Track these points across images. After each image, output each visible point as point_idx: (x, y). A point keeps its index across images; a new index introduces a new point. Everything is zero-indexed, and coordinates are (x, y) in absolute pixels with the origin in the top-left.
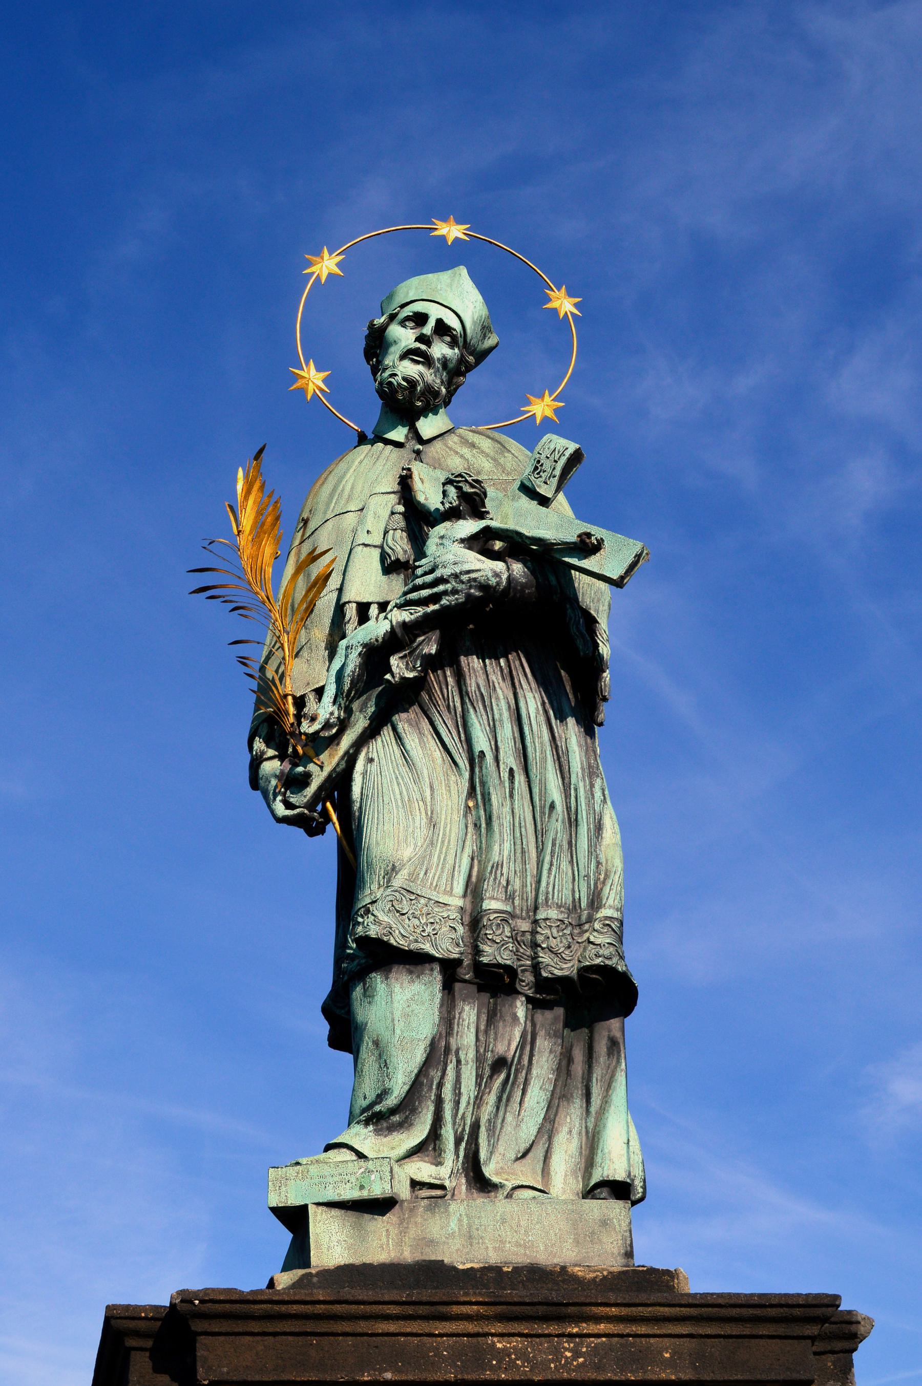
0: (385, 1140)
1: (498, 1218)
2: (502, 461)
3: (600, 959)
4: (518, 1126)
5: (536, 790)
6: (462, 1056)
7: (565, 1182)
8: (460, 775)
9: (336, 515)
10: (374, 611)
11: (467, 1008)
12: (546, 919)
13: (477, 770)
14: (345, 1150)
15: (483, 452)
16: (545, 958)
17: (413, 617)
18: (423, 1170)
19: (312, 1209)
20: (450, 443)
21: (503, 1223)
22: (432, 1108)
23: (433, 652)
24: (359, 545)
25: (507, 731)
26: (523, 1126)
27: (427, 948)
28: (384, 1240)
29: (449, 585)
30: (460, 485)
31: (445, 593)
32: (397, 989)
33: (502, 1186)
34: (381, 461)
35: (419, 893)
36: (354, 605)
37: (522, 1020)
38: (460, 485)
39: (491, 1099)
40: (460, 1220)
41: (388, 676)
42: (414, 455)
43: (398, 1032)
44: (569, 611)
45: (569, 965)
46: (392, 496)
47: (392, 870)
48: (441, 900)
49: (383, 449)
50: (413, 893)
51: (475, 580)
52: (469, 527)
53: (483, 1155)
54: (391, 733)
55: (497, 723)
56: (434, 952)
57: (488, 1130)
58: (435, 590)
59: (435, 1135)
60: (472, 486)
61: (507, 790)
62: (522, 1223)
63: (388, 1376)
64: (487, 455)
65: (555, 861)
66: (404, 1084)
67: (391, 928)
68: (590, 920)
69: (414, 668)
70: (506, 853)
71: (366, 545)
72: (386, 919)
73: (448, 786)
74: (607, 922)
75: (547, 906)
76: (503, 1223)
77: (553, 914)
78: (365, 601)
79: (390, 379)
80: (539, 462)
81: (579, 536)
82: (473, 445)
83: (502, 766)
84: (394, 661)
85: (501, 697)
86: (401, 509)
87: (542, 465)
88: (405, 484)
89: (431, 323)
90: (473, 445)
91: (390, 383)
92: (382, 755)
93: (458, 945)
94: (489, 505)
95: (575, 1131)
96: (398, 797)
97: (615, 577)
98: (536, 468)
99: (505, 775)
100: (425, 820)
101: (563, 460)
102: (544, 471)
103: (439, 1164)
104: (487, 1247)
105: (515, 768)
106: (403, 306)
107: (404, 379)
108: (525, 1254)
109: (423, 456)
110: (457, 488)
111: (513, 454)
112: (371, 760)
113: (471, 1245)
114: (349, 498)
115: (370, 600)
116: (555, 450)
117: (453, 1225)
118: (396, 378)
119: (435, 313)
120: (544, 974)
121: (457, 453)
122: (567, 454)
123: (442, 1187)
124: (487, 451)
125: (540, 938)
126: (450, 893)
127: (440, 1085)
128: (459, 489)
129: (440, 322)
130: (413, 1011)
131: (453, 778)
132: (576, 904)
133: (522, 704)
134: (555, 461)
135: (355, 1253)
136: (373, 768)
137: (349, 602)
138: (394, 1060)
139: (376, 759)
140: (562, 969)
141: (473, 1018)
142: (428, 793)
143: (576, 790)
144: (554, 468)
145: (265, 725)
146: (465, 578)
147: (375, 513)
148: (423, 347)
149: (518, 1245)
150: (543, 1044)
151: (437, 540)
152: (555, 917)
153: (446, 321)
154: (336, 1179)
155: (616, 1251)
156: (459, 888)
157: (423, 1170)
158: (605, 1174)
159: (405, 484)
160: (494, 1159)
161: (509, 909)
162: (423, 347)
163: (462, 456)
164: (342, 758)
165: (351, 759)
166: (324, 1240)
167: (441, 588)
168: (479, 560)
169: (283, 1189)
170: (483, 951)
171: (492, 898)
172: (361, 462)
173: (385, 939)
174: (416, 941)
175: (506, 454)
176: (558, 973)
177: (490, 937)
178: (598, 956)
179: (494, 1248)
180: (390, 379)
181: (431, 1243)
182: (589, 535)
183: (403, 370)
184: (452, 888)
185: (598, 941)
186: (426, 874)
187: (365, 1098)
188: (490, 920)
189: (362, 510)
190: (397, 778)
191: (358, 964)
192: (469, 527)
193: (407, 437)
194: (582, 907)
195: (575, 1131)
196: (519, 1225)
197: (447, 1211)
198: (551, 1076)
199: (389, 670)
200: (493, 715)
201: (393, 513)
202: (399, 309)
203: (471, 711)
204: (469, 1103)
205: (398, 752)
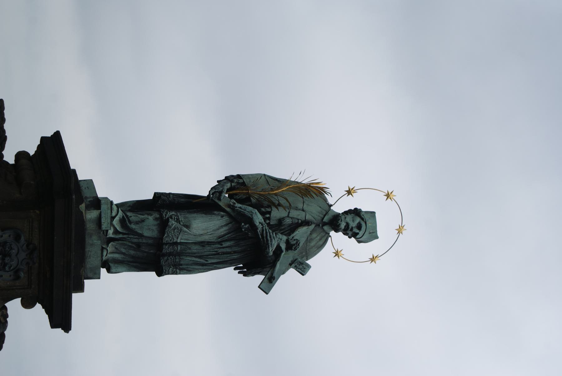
0: (119, 222)
1: (97, 251)
2: (314, 248)
3: (165, 271)
4: (124, 248)
5: (212, 257)
6: (140, 239)
7: (111, 257)
8: (216, 240)
9: (304, 201)
10: (268, 216)
11: (152, 241)
12: (176, 259)
13: (217, 243)
14: (117, 213)
15: (317, 242)
16: (166, 258)
17: (259, 231)
18: (111, 232)
19: (100, 211)
20: (322, 233)
21: (95, 252)
22: (127, 232)
23: (249, 236)
24: (289, 211)
25: (228, 250)
26: (124, 250)
27: (166, 235)
28: (92, 227)
29: (266, 242)
30: (295, 245)
31: (264, 240)
32: (156, 227)
33: (108, 247)
34: (318, 214)
35: (181, 233)
36: (270, 210)
37: (150, 252)
38: (295, 245)
39: (130, 244)
40: (96, 243)
41: (243, 224)
42: (318, 224)
43: (145, 227)
44: (259, 269)
45: (164, 264)
46: (304, 219)
47: (188, 227)
48: (179, 238)
49: (323, 215)
50: (180, 231)
51: (267, 249)
52: (283, 246)
53: (116, 242)
54: (229, 222)
55: (231, 248)
56: (164, 237)
57: (122, 243)
58: (265, 238)
59: (120, 233)
60: (294, 248)
61: (211, 250)
62: (95, 256)
63: (55, 238)
64: (316, 243)
65: (191, 261)
66: (132, 228)
67: (171, 227)
68: (176, 268)
69: (245, 230)
70: (193, 250)
71: (289, 212)
72: (173, 226)
73: (213, 237)
74: (175, 272)
75: (180, 259)
76: (95, 252)
77: (177, 260)
78: (271, 213)
79: (340, 220)
80: (303, 264)
81: (274, 277)
82: (320, 239)
83: (218, 249)
84: (247, 225)
85: (239, 249)
86: (300, 221)
87: (301, 265)
88: (306, 223)
89: (358, 231)
90: (320, 239)
91: (339, 219)
92: (223, 220)
93: (166, 242)
94: (290, 251)
95: (124, 259)
96: (209, 226)
97: (260, 286)
98: (301, 263)
99: (216, 250)
100: (201, 234)
101: (301, 271)
102: (299, 266)
103: (113, 234)
104: (89, 248)
105: (218, 252)
106: (366, 223)
107: (340, 224)
108: (88, 256)
109: (318, 226)
110: (295, 244)
111: (316, 250)
112: (222, 216)
113: (90, 245)
114: (308, 205)
115: (271, 215)
116: (305, 269)
117: (95, 241)
118: (340, 222)
119: (361, 233)
120: (161, 258)
121: (318, 235)
122: (303, 273)
123: (107, 235)
124: (318, 243)
125: (171, 257)
126: (181, 239)
127: (133, 235)
128: (294, 245)
129: (358, 234)
130: (150, 231)
131: (215, 238)
132: (181, 265)
133: (236, 254)
134: (301, 269)
135: (89, 220)
136: (220, 218)
137: (271, 209)
138: (138, 225)
139: (223, 218)
140: (163, 262)
141: (150, 242)
142: (209, 234)
143: (212, 266)
144: (299, 269)
145: (242, 182)
146: (267, 246)
147: (299, 215)
148: (349, 229)
149: (90, 255)
150: (145, 254)
151: (280, 238)
152: (177, 261)
153: (358, 235)
154: (107, 217)
155: (88, 276)
156: (182, 241)
157: (111, 232)
158: (112, 267)
159: (306, 223)
160: (116, 244)
161: (178, 251)
162: (349, 229)
163: (317, 237)
164: (224, 209)
165: (224, 210)
166: (92, 214)
167: (265, 240)
168: (272, 250)
169: (105, 204)
170: (166, 246)
171: (181, 247)
172: (320, 207)
173: (168, 227)
174: (167, 233)
175: (316, 249)
176: (162, 261)
177: (170, 247)
178: (166, 270)
179: (89, 250)
180: (340, 220)
181: (91, 237)
182: (274, 279)
183: (342, 224)
184: (182, 240)
185: (170, 270)
186: (186, 234)
187: (131, 217)
188: (175, 247)
189: (303, 210)
190: (215, 225)
191: (164, 217)
192: (283, 246)
193: (324, 222)
194: (180, 266)
195: (124, 259)
196: (95, 255)
197: (98, 240)
198: (137, 256)
199: (245, 224)
200: (234, 247)
201: (298, 219)
202: (365, 221)
203: (234, 242)
204: (129, 240)
205: (223, 224)
